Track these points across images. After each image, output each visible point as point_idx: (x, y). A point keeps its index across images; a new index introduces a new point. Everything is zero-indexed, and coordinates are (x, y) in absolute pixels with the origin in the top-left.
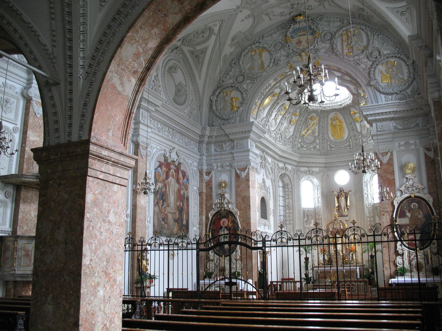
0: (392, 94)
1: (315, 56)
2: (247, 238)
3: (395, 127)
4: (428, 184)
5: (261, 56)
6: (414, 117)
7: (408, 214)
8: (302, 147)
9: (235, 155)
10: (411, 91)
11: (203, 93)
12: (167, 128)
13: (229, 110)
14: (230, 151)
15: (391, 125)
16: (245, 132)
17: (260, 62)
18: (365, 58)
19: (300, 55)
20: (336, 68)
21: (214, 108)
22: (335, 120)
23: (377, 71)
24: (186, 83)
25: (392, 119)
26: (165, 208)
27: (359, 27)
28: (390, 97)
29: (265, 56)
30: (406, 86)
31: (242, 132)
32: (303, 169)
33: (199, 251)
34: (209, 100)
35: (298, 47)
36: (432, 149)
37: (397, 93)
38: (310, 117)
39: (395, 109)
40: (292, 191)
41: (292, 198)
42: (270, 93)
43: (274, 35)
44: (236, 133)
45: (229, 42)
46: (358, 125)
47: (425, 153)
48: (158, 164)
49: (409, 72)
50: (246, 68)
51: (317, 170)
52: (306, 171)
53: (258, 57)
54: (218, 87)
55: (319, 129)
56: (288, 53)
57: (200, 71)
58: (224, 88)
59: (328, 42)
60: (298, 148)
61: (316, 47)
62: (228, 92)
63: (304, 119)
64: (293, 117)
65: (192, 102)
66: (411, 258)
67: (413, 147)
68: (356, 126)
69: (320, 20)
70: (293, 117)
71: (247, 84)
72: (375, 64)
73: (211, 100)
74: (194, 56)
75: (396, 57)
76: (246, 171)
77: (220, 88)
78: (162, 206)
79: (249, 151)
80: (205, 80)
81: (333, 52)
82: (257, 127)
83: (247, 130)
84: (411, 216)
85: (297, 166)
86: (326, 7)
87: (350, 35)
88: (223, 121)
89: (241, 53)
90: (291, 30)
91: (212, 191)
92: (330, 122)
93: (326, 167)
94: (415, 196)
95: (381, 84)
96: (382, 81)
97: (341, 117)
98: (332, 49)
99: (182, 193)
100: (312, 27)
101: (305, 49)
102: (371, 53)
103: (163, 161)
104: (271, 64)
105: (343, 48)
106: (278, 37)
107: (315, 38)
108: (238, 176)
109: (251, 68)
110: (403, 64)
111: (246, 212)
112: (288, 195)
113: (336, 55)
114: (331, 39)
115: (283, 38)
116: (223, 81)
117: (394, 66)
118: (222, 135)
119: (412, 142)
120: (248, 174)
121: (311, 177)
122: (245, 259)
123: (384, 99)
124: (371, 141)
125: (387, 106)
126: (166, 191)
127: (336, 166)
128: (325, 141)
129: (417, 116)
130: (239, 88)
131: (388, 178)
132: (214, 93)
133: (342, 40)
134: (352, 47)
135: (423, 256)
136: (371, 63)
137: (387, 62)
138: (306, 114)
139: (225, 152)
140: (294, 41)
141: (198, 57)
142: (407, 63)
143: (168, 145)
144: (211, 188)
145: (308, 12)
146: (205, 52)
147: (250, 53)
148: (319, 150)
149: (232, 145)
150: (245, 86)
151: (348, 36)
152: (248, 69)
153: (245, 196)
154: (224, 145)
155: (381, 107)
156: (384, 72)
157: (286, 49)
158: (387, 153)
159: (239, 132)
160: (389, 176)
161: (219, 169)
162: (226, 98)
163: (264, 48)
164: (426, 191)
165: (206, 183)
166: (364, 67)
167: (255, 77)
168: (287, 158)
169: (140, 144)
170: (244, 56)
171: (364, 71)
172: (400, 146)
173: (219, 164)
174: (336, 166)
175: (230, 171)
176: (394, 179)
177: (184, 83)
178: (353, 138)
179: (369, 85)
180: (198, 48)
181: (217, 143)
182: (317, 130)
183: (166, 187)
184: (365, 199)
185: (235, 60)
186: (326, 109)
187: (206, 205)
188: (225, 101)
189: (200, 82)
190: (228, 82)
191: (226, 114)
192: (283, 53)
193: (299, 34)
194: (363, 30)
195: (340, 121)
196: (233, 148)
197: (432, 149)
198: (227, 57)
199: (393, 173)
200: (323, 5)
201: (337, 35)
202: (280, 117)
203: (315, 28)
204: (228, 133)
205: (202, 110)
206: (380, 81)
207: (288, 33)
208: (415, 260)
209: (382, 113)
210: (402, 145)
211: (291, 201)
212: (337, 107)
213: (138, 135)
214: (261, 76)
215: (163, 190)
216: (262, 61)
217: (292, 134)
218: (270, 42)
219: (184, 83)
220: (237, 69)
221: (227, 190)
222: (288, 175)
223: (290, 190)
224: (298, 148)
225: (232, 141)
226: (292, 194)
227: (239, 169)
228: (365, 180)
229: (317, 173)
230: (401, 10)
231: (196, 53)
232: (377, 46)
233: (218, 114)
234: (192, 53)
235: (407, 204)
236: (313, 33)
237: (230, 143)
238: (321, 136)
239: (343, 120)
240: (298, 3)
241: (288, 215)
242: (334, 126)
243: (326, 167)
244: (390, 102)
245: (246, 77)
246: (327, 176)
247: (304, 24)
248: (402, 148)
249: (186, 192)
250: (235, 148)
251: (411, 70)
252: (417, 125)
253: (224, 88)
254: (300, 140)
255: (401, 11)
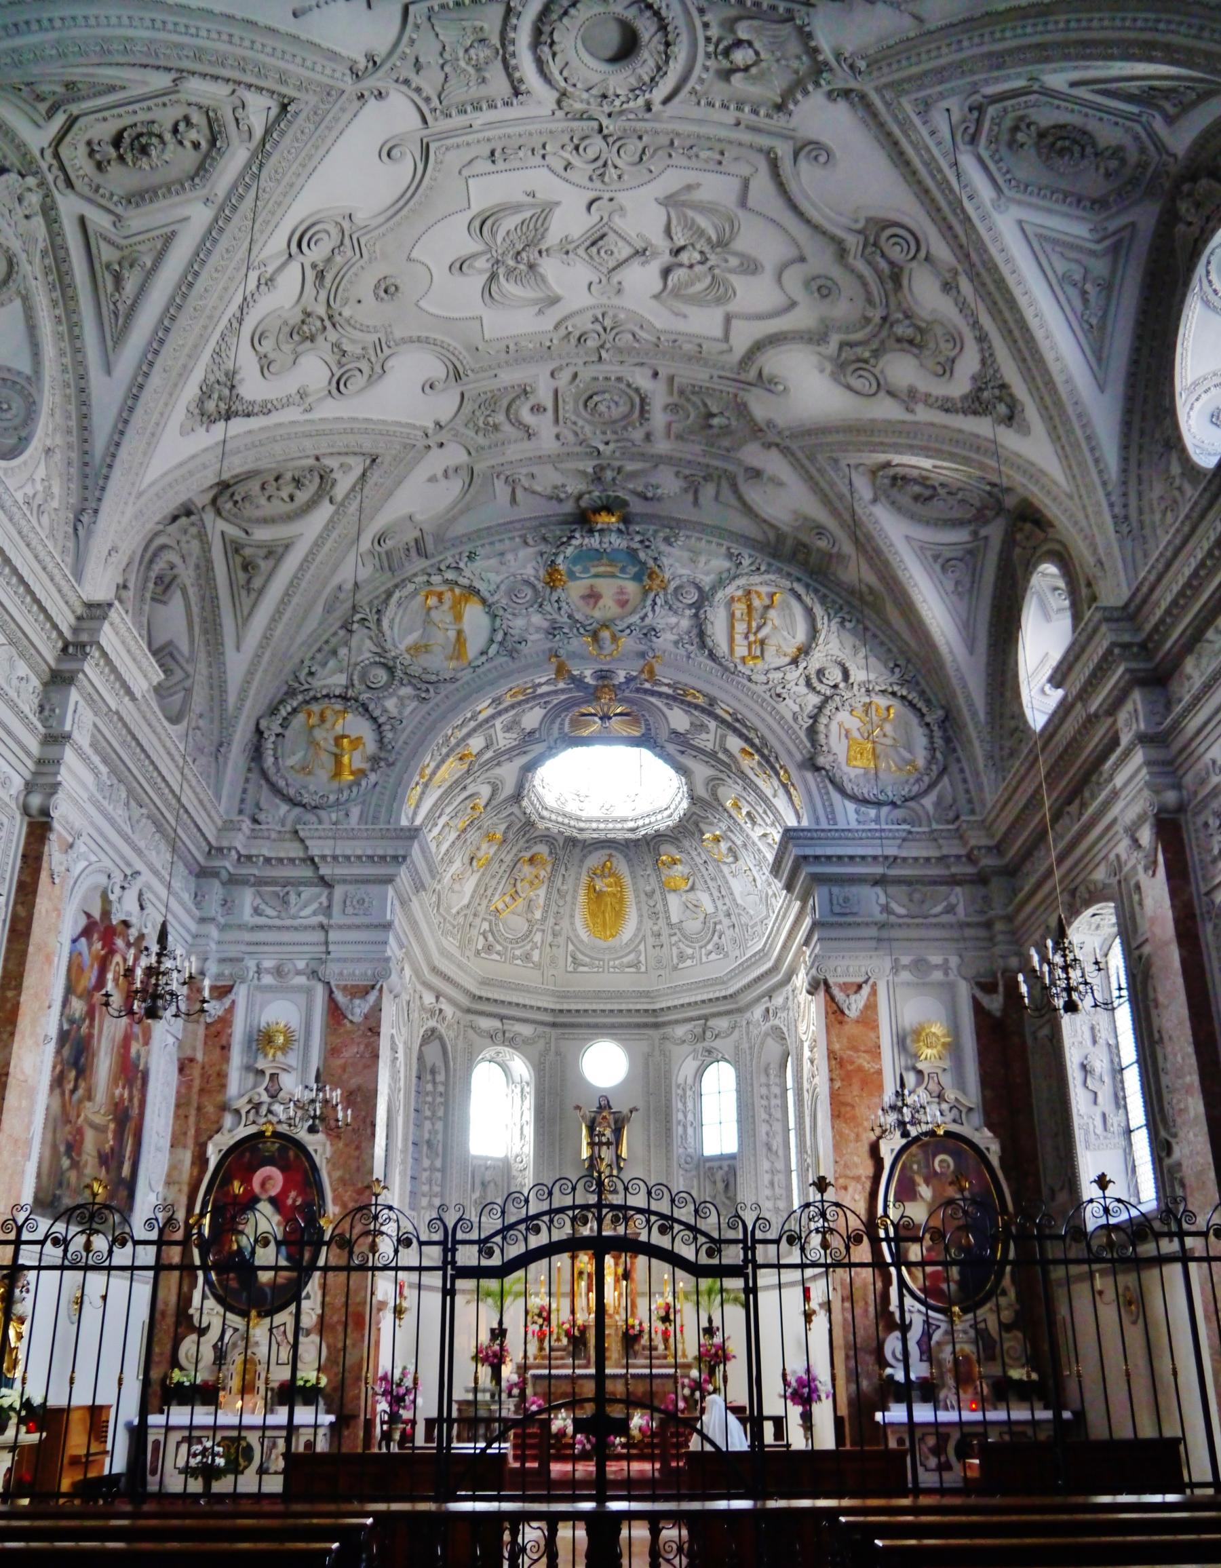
0: (878, 804)
1: (642, 648)
2: (677, 1227)
3: (886, 909)
4: (984, 1097)
5: (458, 617)
6: (941, 883)
7: (925, 1191)
8: (489, 948)
9: (333, 936)
10: (938, 804)
11: (242, 699)
12: (124, 795)
13: (323, 775)
14: (315, 920)
15: (872, 900)
16: (383, 858)
17: (452, 634)
18: (802, 681)
19: (595, 636)
20: (701, 701)
21: (269, 761)
22: (603, 876)
23: (834, 727)
24: (192, 651)
25: (880, 881)
26: (80, 1101)
27: (788, 584)
28: (872, 812)
29: (475, 618)
30: (924, 786)
31: (371, 858)
32: (486, 1024)
33: (453, 1278)
34: (252, 727)
35: (588, 611)
36: (1001, 989)
37: (893, 804)
38: (527, 855)
39: (891, 851)
40: (444, 1095)
41: (445, 1119)
42: (456, 749)
43: (510, 557)
44: (348, 858)
45: (365, 543)
46: (674, 901)
47: (974, 999)
48: (83, 922)
49: (932, 749)
50: (402, 647)
51: (526, 1030)
52: (496, 1030)
53: (449, 618)
54: (291, 693)
55: (548, 899)
56: (554, 621)
57: (243, 621)
58: (315, 699)
59: (688, 612)
60: (478, 952)
61: (648, 621)
62: (328, 713)
63: (508, 859)
64: (484, 846)
65: (201, 723)
66: (937, 1336)
67: (938, 975)
68: (666, 905)
69: (667, 540)
70: (484, 846)
71: (401, 699)
72: (831, 706)
73: (259, 732)
74: (238, 560)
75: (894, 694)
76: (372, 997)
77: (294, 697)
78: (73, 1091)
79: (387, 926)
80: (258, 656)
81: (703, 645)
82: (424, 850)
83: (391, 852)
84: (934, 1197)
85: (469, 1011)
86: (702, 500)
87: (757, 603)
88: (298, 810)
89: (389, 595)
90: (569, 551)
91: (226, 1059)
92: (584, 879)
93: (554, 1025)
94: (947, 1133)
95: (845, 768)
96: (848, 760)
97: (622, 867)
98: (701, 635)
99: (134, 1047)
100: (642, 555)
101: (612, 620)
102: (820, 673)
103: (97, 915)
104: (494, 647)
105: (731, 640)
106: (525, 563)
107: (646, 592)
108: (335, 1012)
109: (418, 649)
110: (914, 721)
111: (358, 1148)
112: (432, 1104)
113: (712, 656)
114: (698, 606)
115: (542, 573)
116: (311, 674)
117: (886, 719)
118: (292, 860)
119: (936, 959)
120: (377, 1009)
121: (507, 1052)
122: (340, 1328)
123: (852, 816)
124: (713, 956)
125: (879, 836)
126: (90, 1036)
127: (588, 1026)
128: (561, 940)
129: (953, 881)
130: (371, 707)
131: (860, 1069)
132: (273, 711)
133: (733, 615)
134: (762, 643)
135: (972, 1333)
136: (814, 700)
137: (867, 707)
138: (521, 843)
139: (297, 922)
140: (575, 590)
141: (249, 566)
142: (928, 719)
143: (123, 857)
144: (225, 1048)
145: (636, 506)
146: (282, 556)
147: (420, 598)
148: (538, 966)
149: (324, 899)
150: (391, 704)
151: (749, 607)
152: (408, 650)
153: (359, 1088)
154: (293, 898)
155: (845, 835)
156: (856, 734)
157: (548, 608)
158: (860, 987)
159: (359, 857)
160: (864, 1061)
161: (268, 979)
162: (319, 734)
163: (473, 591)
164: (977, 1118)
165: (208, 1025)
166: (796, 708)
167: (433, 678)
168: (447, 979)
169: (56, 825)
170: (399, 605)
171: (795, 719)
172: (896, 969)
173: (268, 964)
174: (588, 1026)
175: (309, 991)
176: (879, 1072)
177: (184, 647)
178: (651, 940)
179: (811, 764)
180: (262, 534)
181: (266, 884)
182: (541, 901)
183: (92, 1020)
184: (677, 1141)
185: (357, 615)
186: (586, 835)
187: (199, 1109)
188: (313, 743)
189: (236, 663)
190: (329, 681)
191: (312, 788)
192: (537, 619)
193: (594, 571)
194: (799, 597)
195: (619, 883)
196: (328, 910)
197: (1001, 989)
198: (342, 596)
199: (875, 1052)
200: (696, 492)
201: (720, 595)
202: (454, 835)
203: (651, 563)
204: (315, 851)
205: (226, 758)
206: (842, 758)
207: (560, 560)
208: (949, 1348)
209: (863, 858)
210: (905, 967)
211: (439, 1126)
212: (620, 836)
213: (54, 787)
214: (453, 680)
215: (84, 1029)
216: (459, 633)
217: (465, 901)
218: (495, 578)
219: (184, 646)
220: (368, 643)
221: (292, 1059)
222: (441, 1039)
223: (441, 1088)
224: (478, 952)
225: (325, 883)
226: (446, 1104)
227: (345, 989)
228: (681, 1080)
229: (527, 1042)
230: (948, 554)
231: (247, 552)
232: (836, 652)
233: (281, 783)
234: (234, 548)
235: (921, 1156)
236: (645, 574)
237: (316, 890)
238: (551, 921)
239: (627, 880)
240: (620, 470)
241: (426, 1174)
242: (597, 896)
243: (554, 1025)
244: (873, 826)
245: (399, 673)
246: (558, 1053)
247: (617, 542)
248: (905, 976)
249: (143, 1051)
250: (336, 909)
251: (939, 742)
252: (950, 909)
253: (315, 699)
254: (486, 926)
255: (949, 555)
